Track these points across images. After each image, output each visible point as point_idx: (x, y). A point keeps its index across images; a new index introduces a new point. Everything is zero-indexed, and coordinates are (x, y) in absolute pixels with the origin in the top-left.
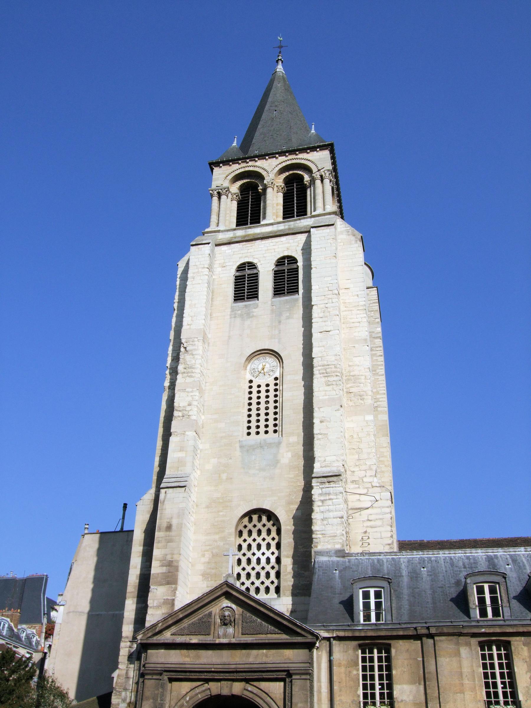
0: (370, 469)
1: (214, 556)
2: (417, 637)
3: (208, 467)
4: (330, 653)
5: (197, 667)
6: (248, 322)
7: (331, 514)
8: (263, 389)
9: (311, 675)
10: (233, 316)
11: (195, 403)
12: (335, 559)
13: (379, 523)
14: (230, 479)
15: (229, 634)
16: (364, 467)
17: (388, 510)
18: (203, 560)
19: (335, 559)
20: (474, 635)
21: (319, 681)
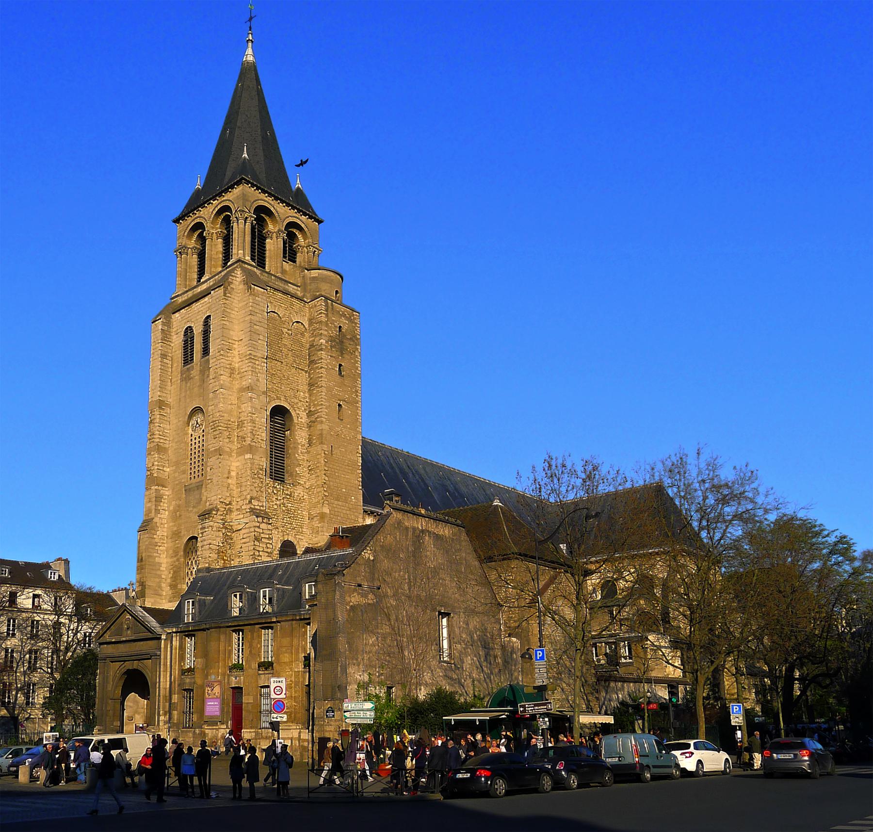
0: (246, 499)
1: (174, 572)
2: (204, 630)
3: (171, 508)
4: (171, 643)
5: (117, 655)
6: (189, 384)
7: (205, 543)
8: (198, 440)
9: (160, 656)
10: (182, 381)
11: (156, 463)
12: (205, 574)
13: (247, 540)
14: (180, 516)
15: (129, 635)
16: (243, 498)
17: (252, 530)
18: (171, 575)
19: (205, 574)
20: (228, 627)
21: (166, 658)
